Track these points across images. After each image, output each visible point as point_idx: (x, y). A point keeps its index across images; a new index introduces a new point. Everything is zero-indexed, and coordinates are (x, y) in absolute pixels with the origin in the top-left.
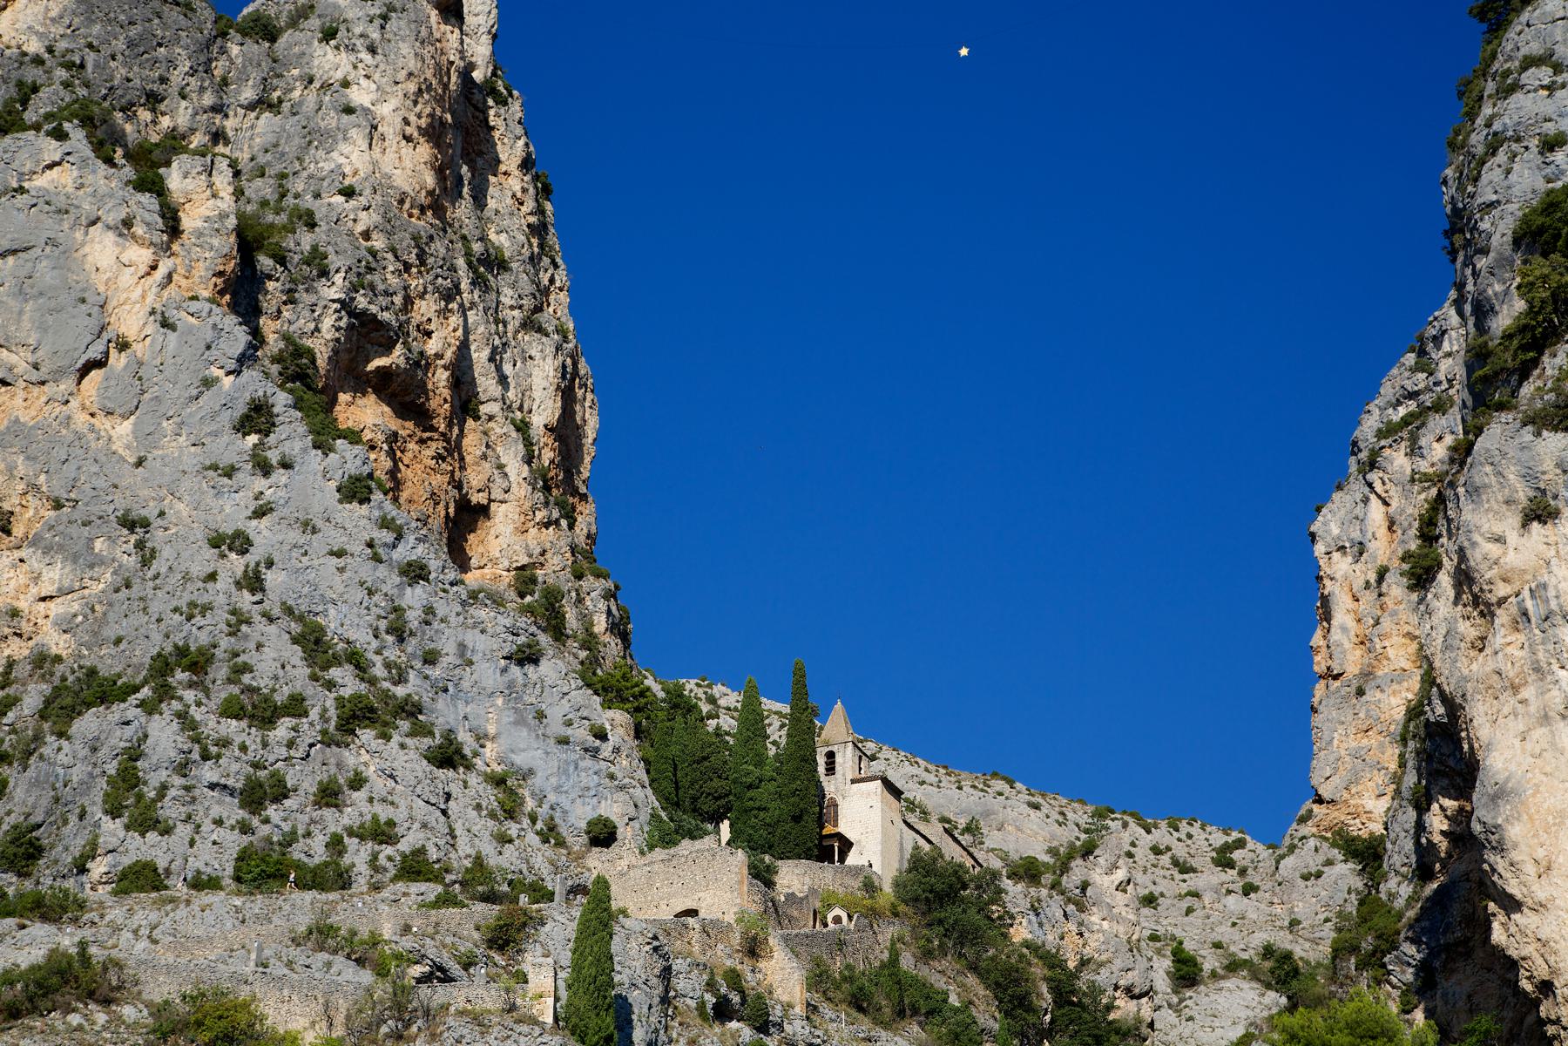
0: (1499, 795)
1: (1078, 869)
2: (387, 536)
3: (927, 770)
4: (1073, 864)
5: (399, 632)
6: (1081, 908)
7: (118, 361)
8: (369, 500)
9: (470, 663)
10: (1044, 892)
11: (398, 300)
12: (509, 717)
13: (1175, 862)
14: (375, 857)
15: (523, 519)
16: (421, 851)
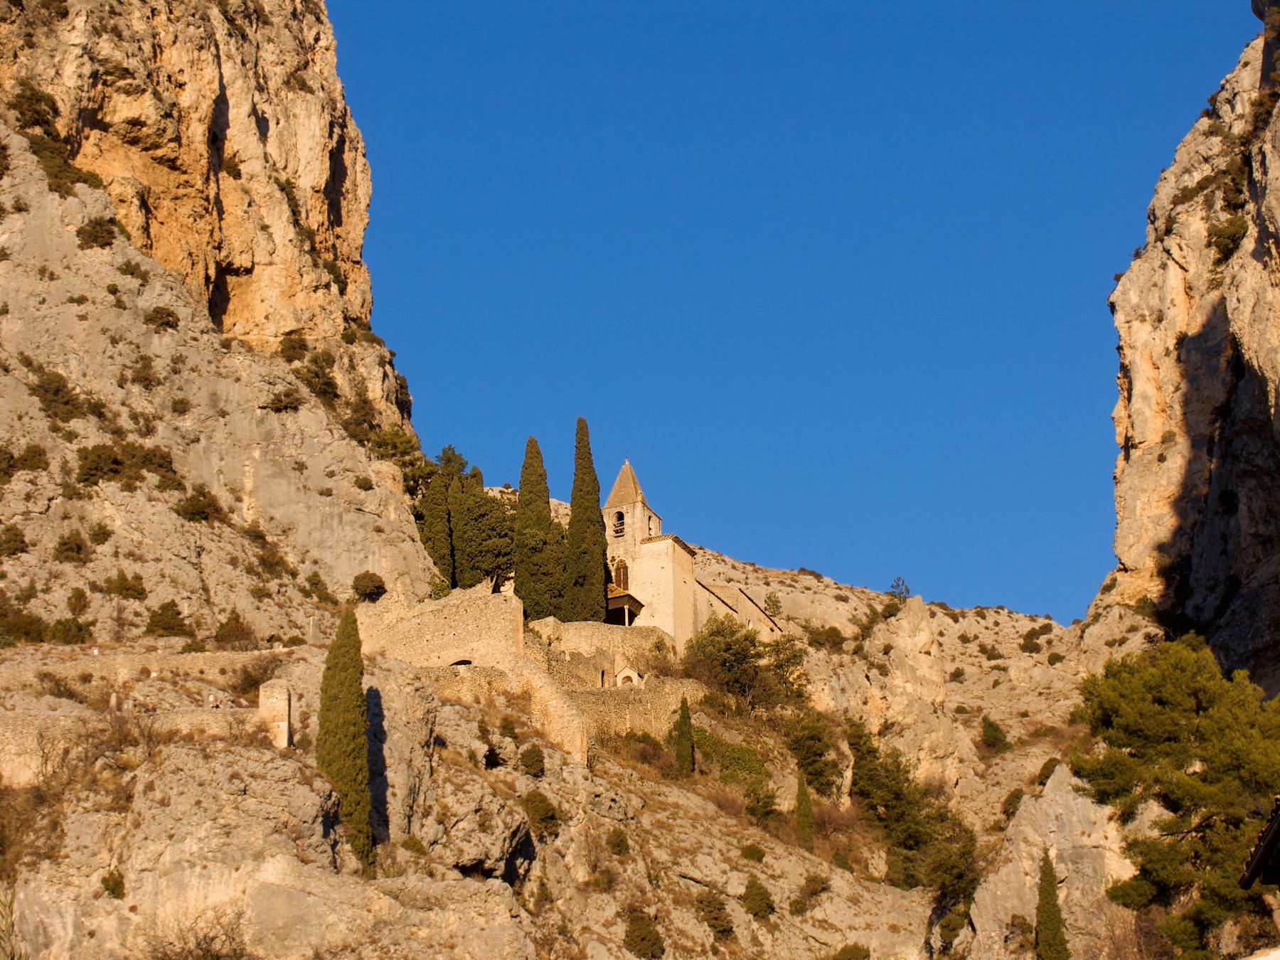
2: (132, 283)
3: (734, 567)
4: (876, 629)
5: (146, 380)
6: (884, 671)
8: (110, 244)
9: (223, 414)
10: (846, 658)
11: (147, 47)
12: (267, 470)
13: (983, 649)
14: (121, 610)
15: (290, 283)
16: (173, 604)
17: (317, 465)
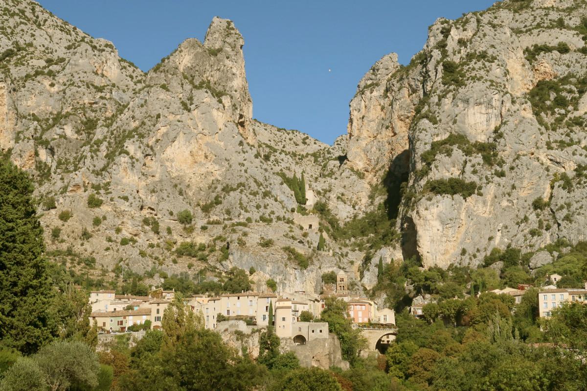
0: (419, 237)
1: (328, 194)
2: (261, 164)
5: (266, 180)
7: (220, 132)
13: (294, 143)
17: (287, 192)
